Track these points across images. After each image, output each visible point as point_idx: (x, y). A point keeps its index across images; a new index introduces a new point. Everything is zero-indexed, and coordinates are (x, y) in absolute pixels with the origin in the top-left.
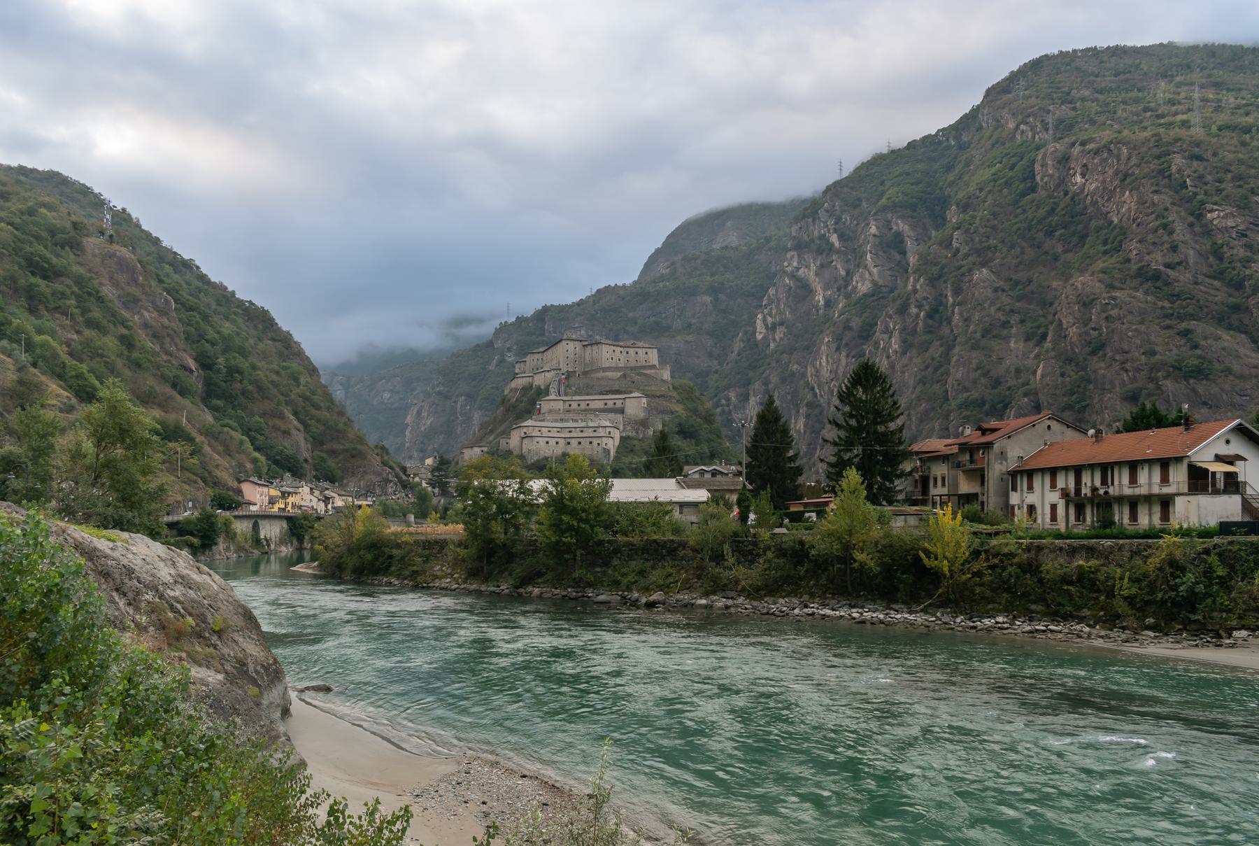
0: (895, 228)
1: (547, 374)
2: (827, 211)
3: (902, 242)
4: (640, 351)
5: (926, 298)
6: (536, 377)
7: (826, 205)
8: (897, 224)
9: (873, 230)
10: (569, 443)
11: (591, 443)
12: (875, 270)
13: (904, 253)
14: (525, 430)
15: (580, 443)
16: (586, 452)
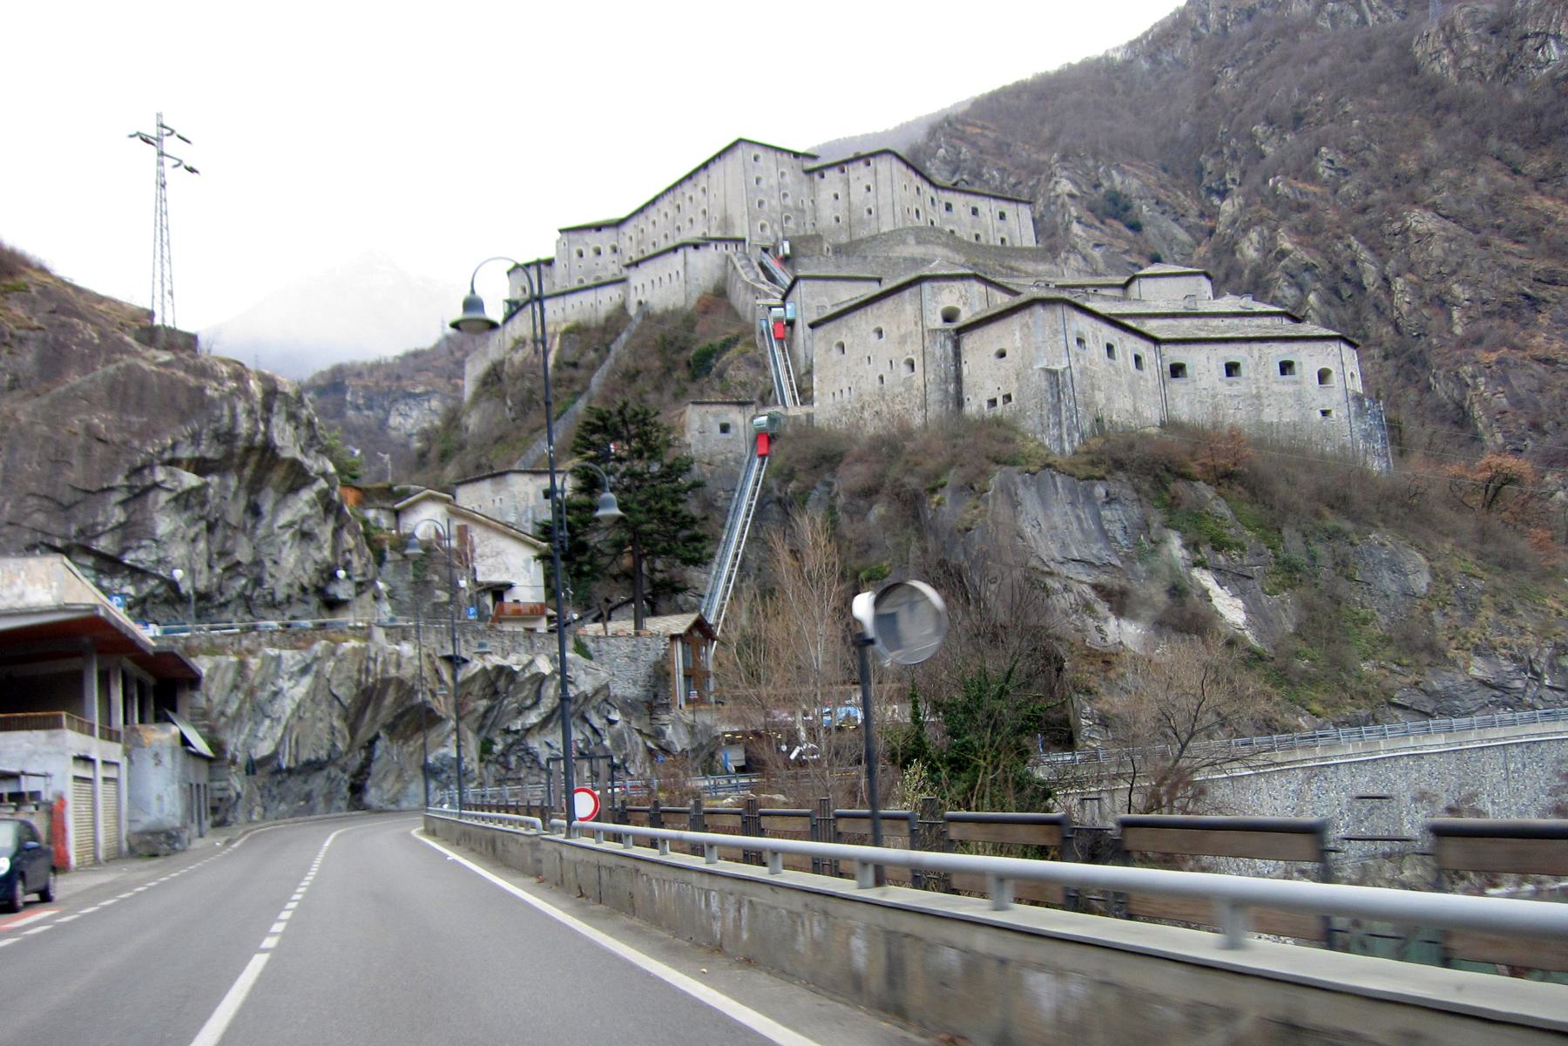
0: (1106, 184)
1: (690, 251)
2: (945, 161)
3: (1127, 208)
4: (983, 205)
5: (1309, 268)
6: (637, 277)
7: (942, 152)
8: (1109, 177)
9: (1066, 186)
10: (1177, 370)
11: (1286, 367)
12: (1097, 253)
13: (1136, 227)
14: (949, 296)
15: (1232, 369)
16: (1269, 415)
